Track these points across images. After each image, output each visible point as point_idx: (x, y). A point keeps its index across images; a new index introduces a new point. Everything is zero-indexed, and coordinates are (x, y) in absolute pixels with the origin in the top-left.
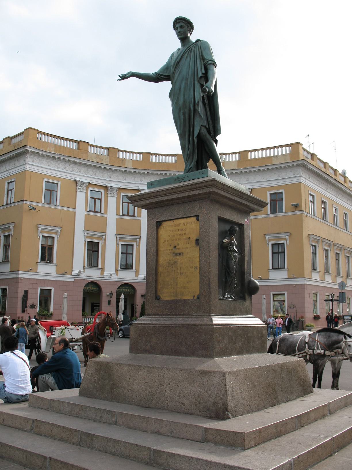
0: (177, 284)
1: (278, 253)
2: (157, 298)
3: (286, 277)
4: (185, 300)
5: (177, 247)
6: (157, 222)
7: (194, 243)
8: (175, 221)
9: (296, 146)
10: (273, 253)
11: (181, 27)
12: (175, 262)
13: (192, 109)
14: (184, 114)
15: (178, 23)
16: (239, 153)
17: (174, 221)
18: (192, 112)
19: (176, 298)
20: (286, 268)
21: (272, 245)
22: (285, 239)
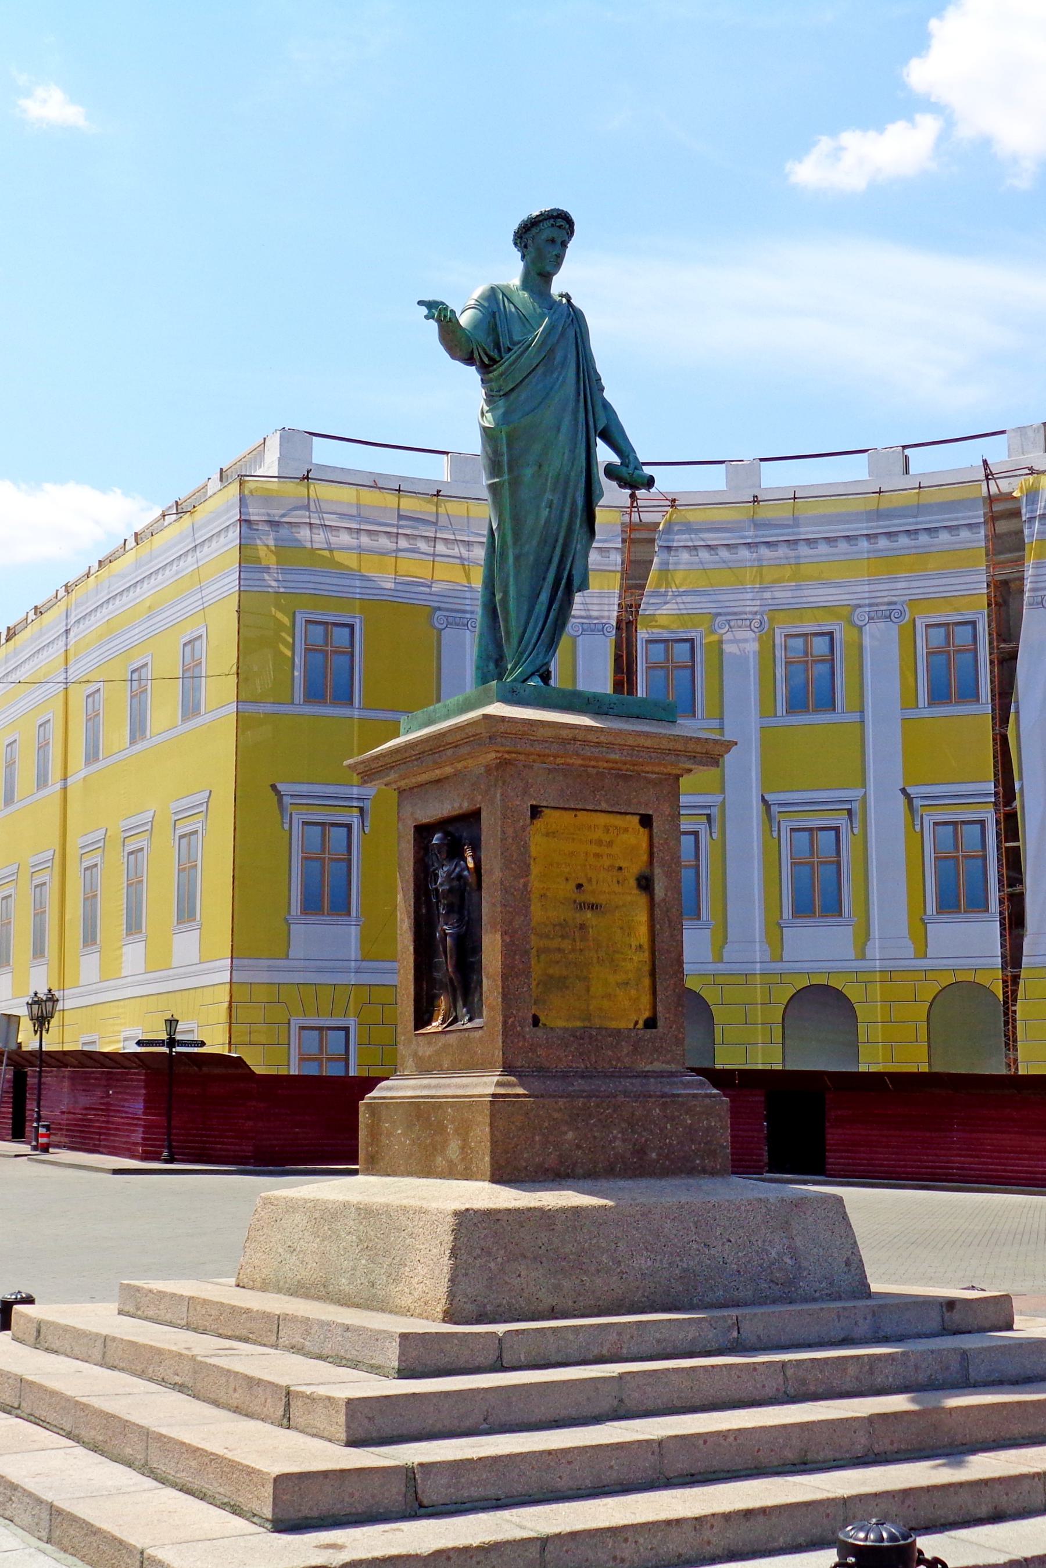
2: (536, 1021)
4: (619, 1031)
6: (532, 806)
7: (633, 883)
17: (578, 813)
19: (587, 1024)
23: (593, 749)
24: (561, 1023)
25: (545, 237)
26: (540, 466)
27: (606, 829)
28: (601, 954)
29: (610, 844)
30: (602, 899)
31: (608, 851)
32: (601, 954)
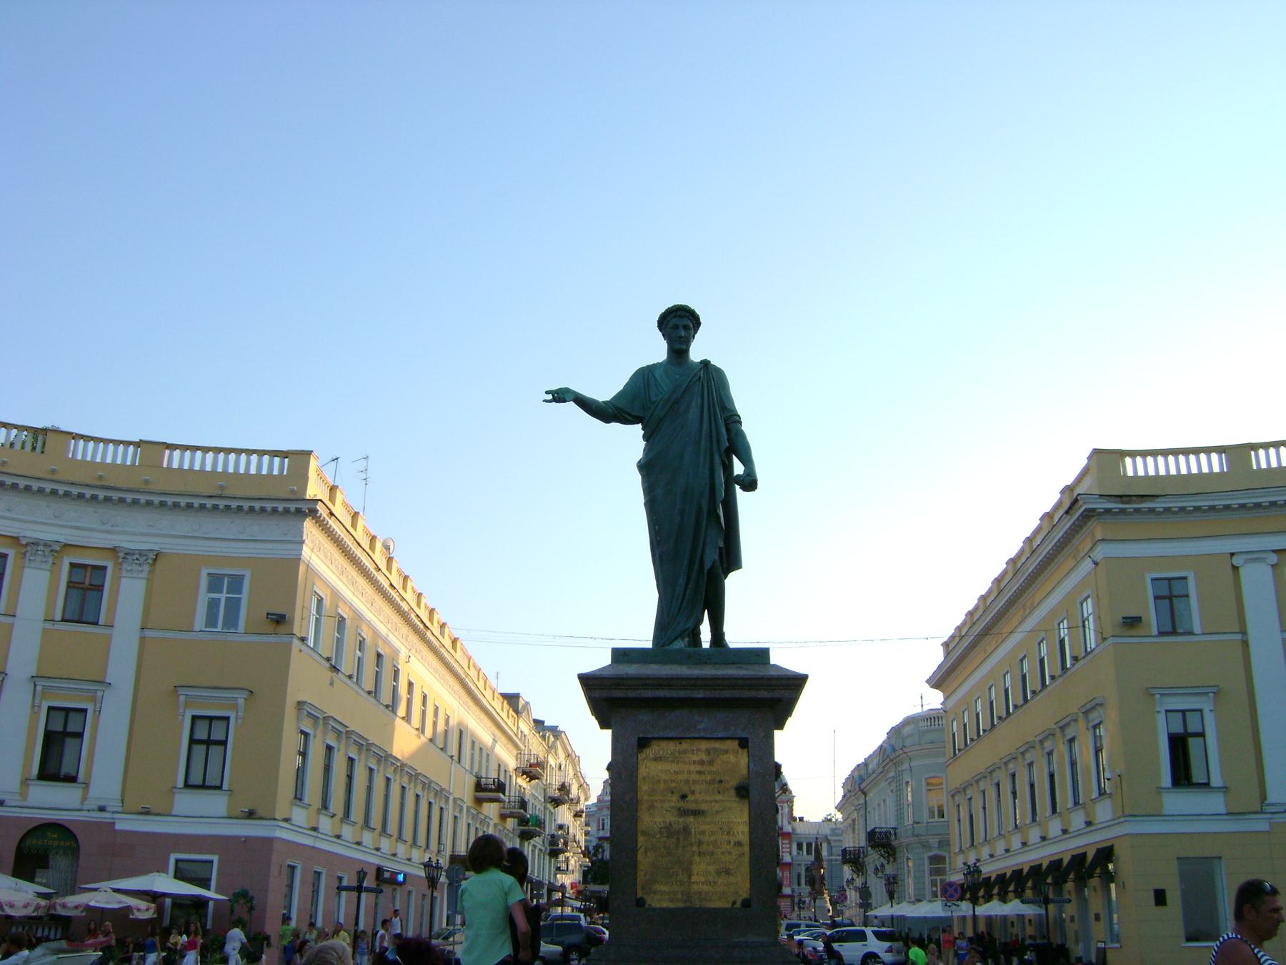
0: (690, 876)
1: (209, 742)
2: (640, 903)
3: (223, 811)
4: (717, 911)
5: (690, 798)
7: (733, 792)
8: (685, 745)
9: (300, 459)
10: (192, 741)
11: (686, 327)
12: (686, 830)
13: (705, 509)
15: (681, 316)
16: (138, 444)
20: (225, 786)
21: (194, 718)
22: (235, 707)
24: (665, 905)
25: (678, 324)
27: (708, 752)
28: (704, 848)
29: (711, 763)
30: (704, 807)
32: (704, 848)
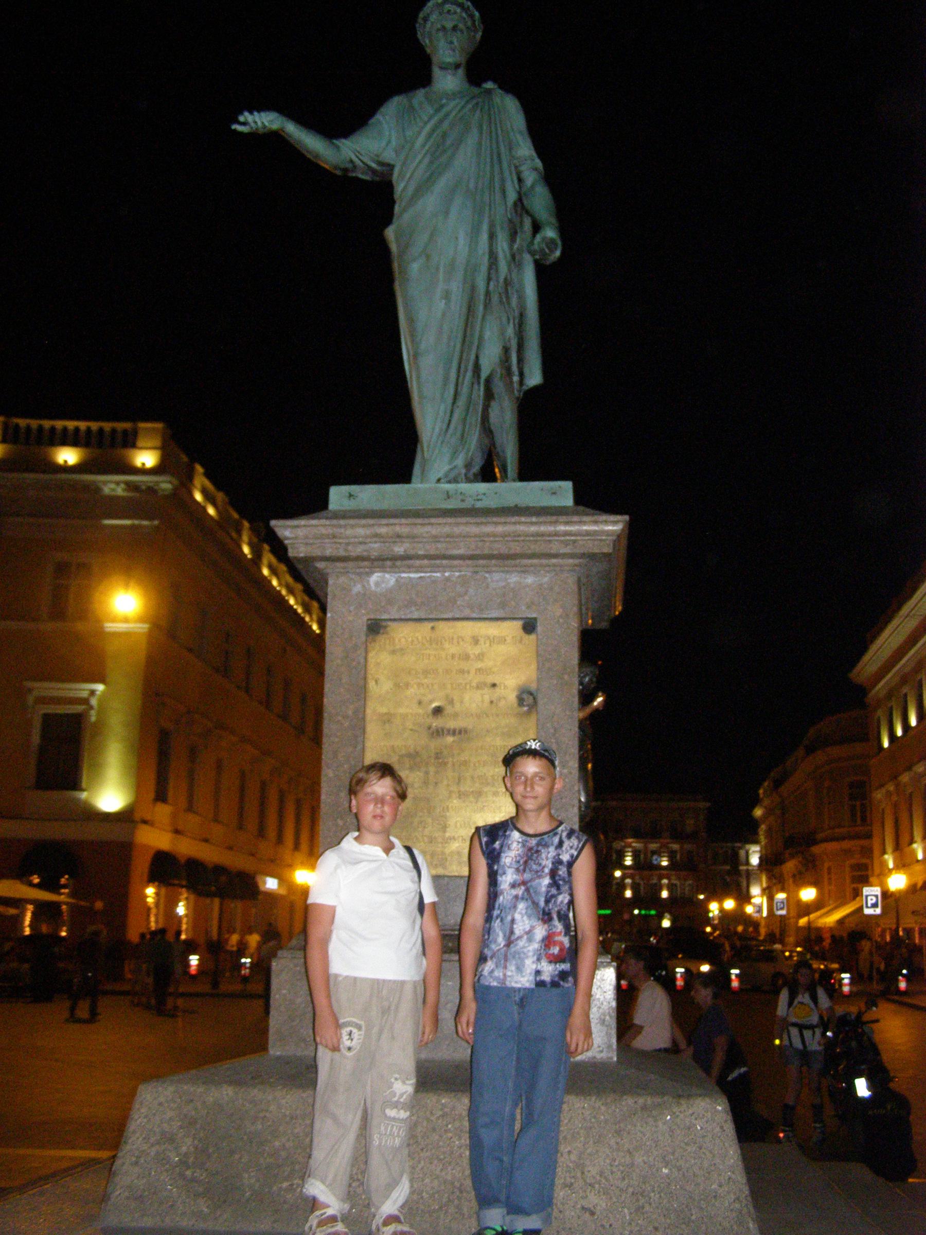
0: (444, 828)
5: (449, 710)
14: (447, 296)
18: (482, 297)
23: (428, 547)
26: (428, 257)
31: (479, 665)
